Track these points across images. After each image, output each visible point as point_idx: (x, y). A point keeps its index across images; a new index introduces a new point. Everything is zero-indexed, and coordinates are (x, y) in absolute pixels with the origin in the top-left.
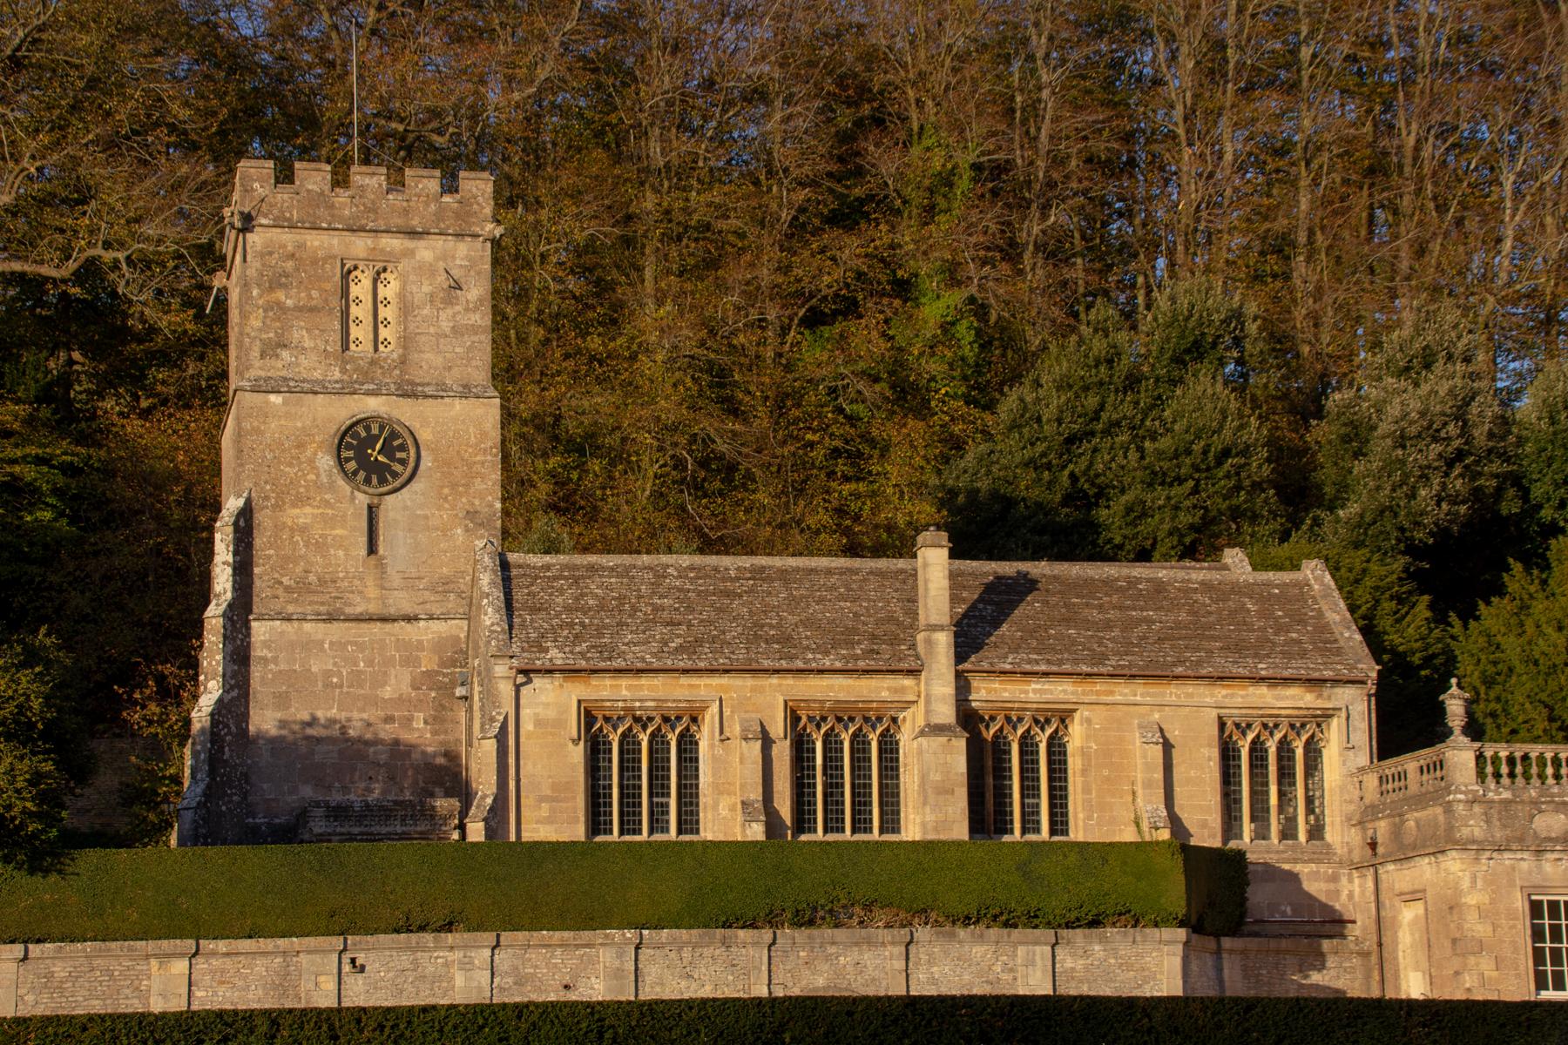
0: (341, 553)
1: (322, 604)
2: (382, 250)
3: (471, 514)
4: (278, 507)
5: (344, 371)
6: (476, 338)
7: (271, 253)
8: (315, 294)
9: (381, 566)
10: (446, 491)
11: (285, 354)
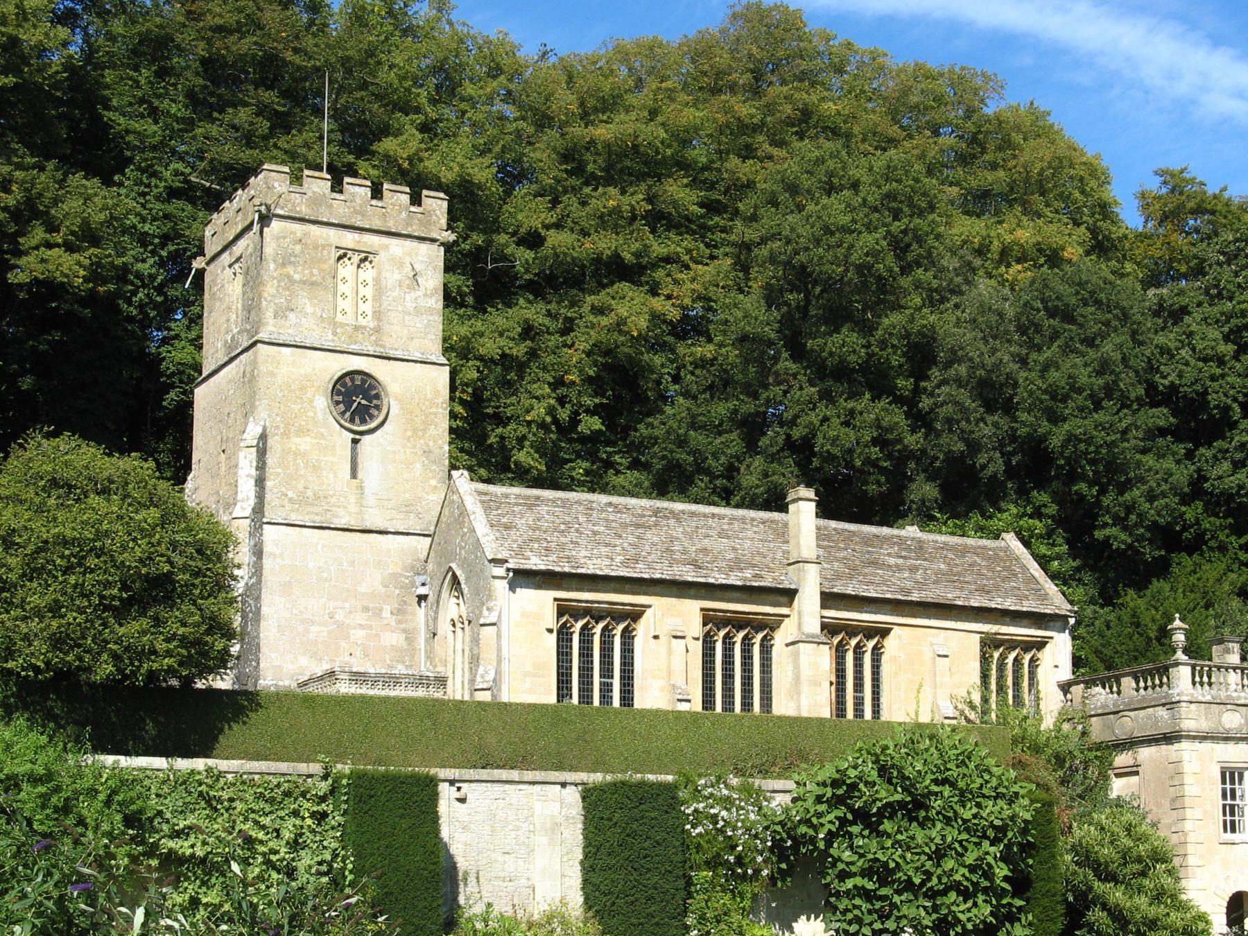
0: (331, 475)
1: (317, 514)
2: (365, 243)
3: (427, 452)
4: (286, 434)
5: (335, 334)
6: (431, 318)
7: (284, 238)
8: (315, 271)
9: (361, 487)
10: (409, 433)
11: (291, 316)
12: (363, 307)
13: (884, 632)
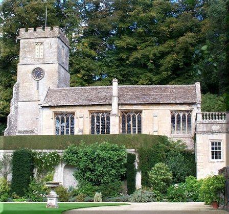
9: (39, 92)
12: (38, 54)
13: (141, 112)
